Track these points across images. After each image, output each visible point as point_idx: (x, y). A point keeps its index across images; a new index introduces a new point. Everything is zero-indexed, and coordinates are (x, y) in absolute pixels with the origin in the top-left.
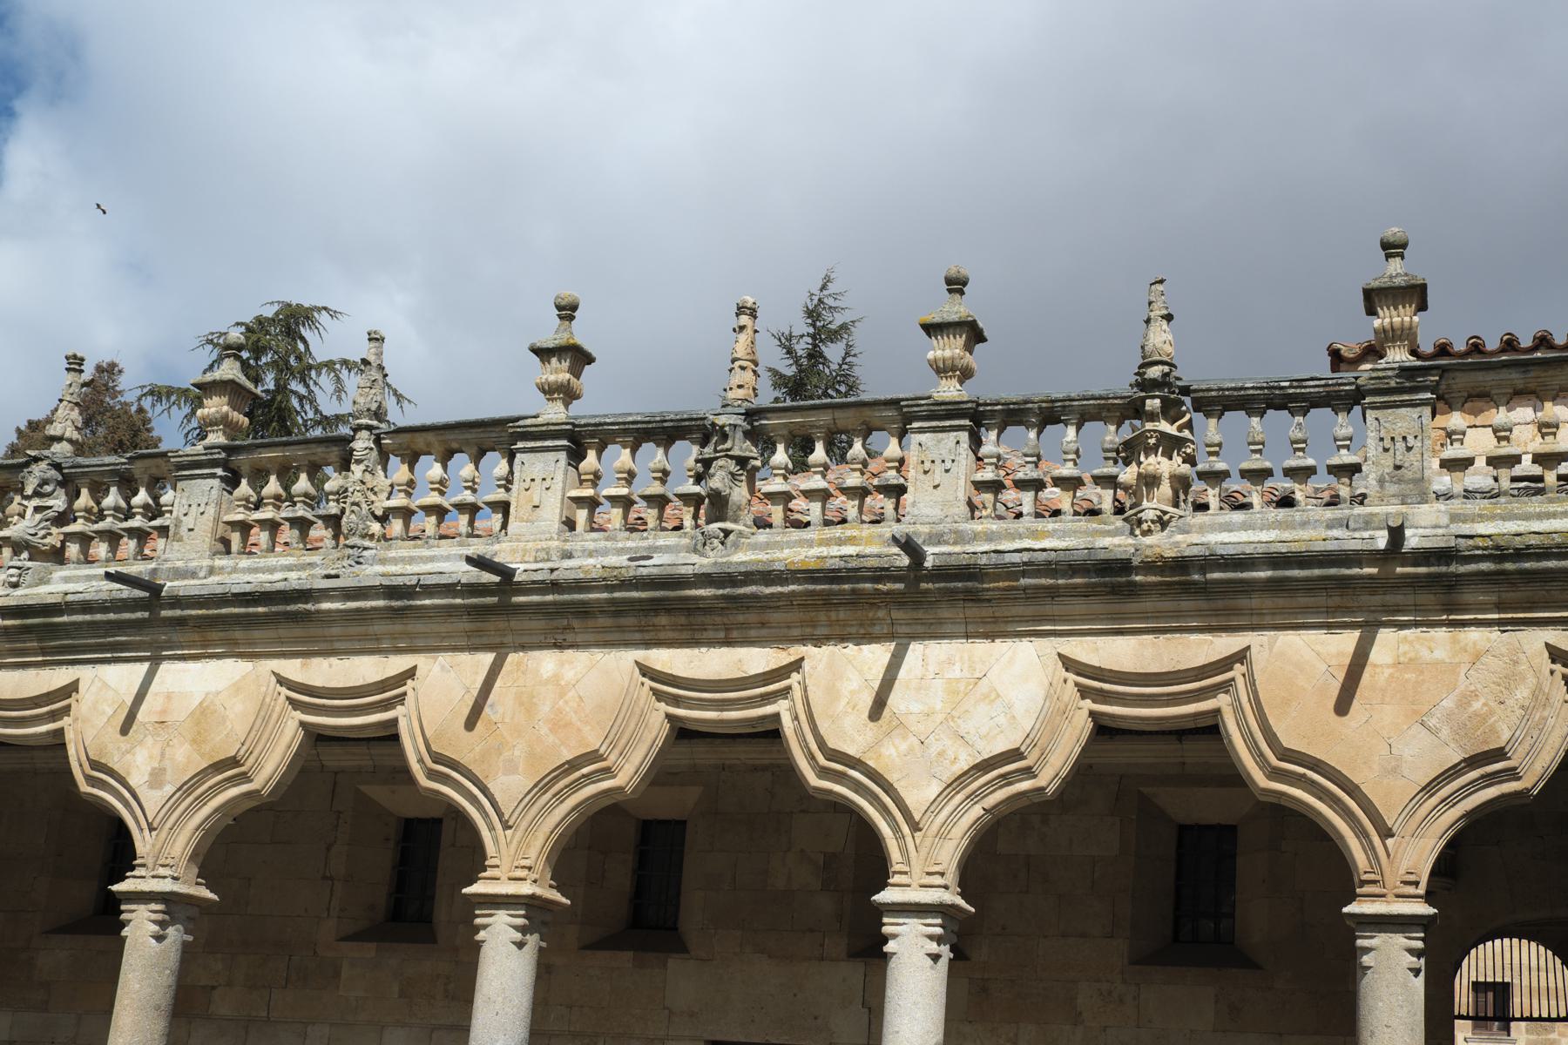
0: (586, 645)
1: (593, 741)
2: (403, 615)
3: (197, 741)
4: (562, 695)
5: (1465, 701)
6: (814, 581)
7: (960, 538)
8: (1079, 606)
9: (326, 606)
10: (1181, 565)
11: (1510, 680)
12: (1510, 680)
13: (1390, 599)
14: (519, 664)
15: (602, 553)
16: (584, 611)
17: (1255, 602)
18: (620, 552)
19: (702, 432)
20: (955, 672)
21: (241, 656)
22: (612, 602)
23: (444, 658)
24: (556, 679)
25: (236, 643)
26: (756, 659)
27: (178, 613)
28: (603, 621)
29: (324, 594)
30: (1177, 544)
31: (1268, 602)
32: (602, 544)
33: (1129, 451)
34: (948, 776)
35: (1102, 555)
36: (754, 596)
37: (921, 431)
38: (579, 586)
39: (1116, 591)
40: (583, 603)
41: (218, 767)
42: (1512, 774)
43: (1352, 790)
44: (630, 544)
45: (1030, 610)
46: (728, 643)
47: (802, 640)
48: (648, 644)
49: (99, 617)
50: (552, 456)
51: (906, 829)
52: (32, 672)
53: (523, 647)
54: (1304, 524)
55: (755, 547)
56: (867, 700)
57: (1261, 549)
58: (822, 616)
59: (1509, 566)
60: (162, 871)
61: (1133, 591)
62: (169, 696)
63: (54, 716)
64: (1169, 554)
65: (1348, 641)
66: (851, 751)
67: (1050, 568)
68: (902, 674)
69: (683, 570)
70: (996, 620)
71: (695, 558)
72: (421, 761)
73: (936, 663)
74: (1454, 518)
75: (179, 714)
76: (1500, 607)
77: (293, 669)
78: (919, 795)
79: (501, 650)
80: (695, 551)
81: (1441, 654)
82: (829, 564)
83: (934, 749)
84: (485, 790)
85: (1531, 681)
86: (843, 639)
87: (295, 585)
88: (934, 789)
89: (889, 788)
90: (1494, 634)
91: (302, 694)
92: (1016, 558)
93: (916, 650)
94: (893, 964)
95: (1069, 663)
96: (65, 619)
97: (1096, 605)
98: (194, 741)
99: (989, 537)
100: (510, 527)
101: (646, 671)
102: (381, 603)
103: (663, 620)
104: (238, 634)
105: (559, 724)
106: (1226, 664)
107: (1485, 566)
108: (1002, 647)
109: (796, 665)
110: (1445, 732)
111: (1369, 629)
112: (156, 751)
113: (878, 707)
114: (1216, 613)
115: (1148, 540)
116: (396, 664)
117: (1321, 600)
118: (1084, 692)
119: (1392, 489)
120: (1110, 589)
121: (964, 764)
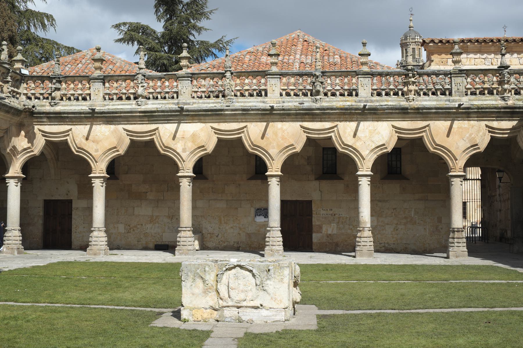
0: (288, 121)
1: (292, 142)
2: (246, 114)
3: (193, 142)
4: (283, 132)
5: (471, 135)
6: (342, 110)
7: (372, 101)
8: (396, 116)
9: (226, 112)
10: (418, 109)
11: (479, 131)
12: (479, 131)
13: (457, 116)
14: (272, 125)
15: (292, 103)
16: (289, 115)
17: (431, 116)
18: (296, 102)
19: (310, 75)
20: (371, 128)
21: (202, 122)
22: (296, 113)
23: (254, 124)
24: (282, 128)
25: (201, 120)
26: (327, 125)
27: (187, 113)
28: (293, 117)
29: (227, 110)
30: (417, 105)
31: (434, 116)
32: (291, 100)
33: (406, 84)
34: (370, 149)
35: (403, 107)
36: (329, 113)
37: (361, 77)
38: (289, 110)
39: (404, 113)
40: (289, 113)
41: (199, 148)
42: (479, 148)
43: (450, 151)
44: (297, 100)
45: (387, 116)
46: (321, 121)
47: (337, 121)
48: (302, 121)
49: (166, 114)
50: (276, 79)
51: (362, 160)
52: (145, 125)
53: (273, 122)
54: (441, 100)
55: (326, 101)
56: (352, 134)
57: (434, 106)
58: (342, 116)
59: (480, 110)
60: (187, 171)
61: (408, 113)
62: (184, 132)
63: (151, 135)
64: (416, 107)
65: (449, 123)
66: (350, 144)
67: (392, 109)
68: (359, 128)
69: (313, 107)
70: (379, 118)
71: (314, 104)
72: (250, 146)
73: (366, 126)
74: (469, 100)
75: (188, 135)
76: (477, 117)
77: (215, 125)
78: (365, 153)
79: (268, 122)
80: (314, 102)
81: (466, 126)
82: (346, 107)
83: (367, 144)
84: (267, 152)
85: (483, 131)
86: (346, 121)
87: (220, 108)
88: (368, 152)
89: (358, 151)
90: (476, 122)
91: (217, 131)
92: (385, 107)
93: (362, 124)
94: (361, 186)
95: (393, 127)
96: (157, 114)
97: (400, 116)
98: (192, 142)
99: (377, 101)
100: (268, 95)
101: (302, 127)
102: (241, 112)
103: (307, 117)
104: (202, 118)
105: (283, 138)
106: (425, 127)
107: (475, 110)
108: (380, 123)
109: (336, 126)
110: (467, 141)
111: (453, 121)
112: (183, 144)
113: (355, 135)
114: (423, 117)
115: (411, 103)
116: (242, 125)
117: (444, 116)
118: (396, 132)
119: (457, 94)
120: (403, 113)
121: (374, 147)
